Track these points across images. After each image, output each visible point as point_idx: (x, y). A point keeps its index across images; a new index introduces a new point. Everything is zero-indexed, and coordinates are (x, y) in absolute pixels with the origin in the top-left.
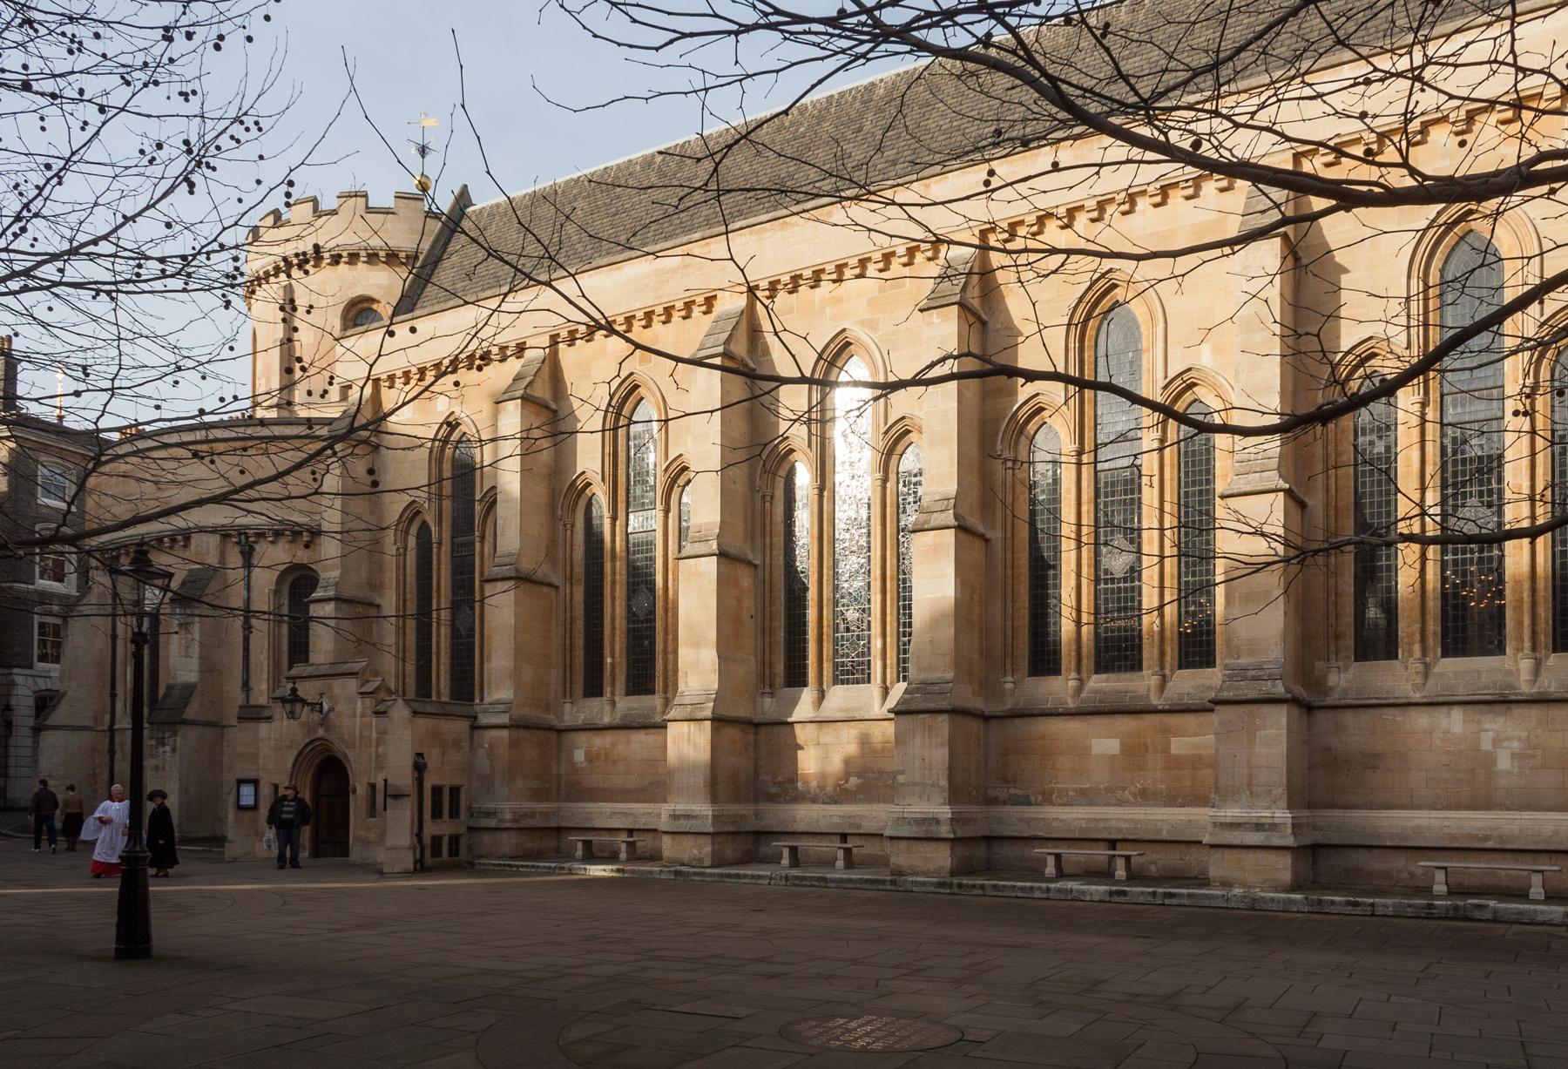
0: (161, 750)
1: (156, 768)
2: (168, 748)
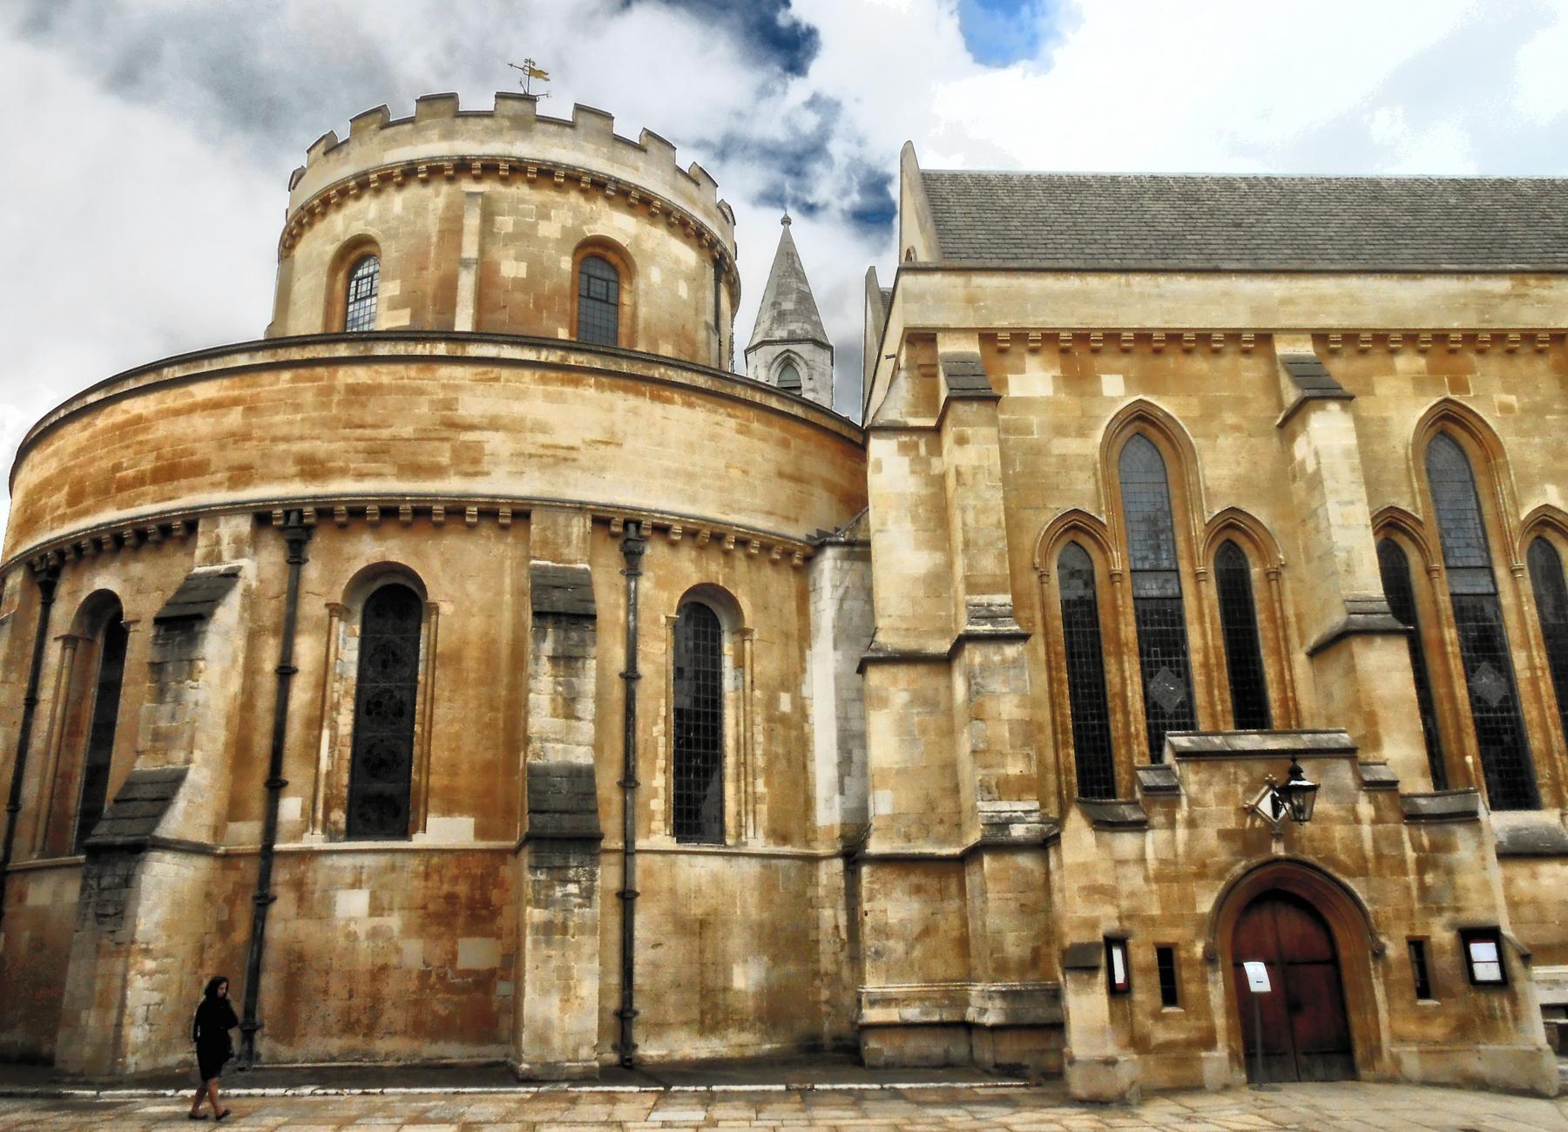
0: (558, 892)
1: (548, 930)
2: (572, 888)
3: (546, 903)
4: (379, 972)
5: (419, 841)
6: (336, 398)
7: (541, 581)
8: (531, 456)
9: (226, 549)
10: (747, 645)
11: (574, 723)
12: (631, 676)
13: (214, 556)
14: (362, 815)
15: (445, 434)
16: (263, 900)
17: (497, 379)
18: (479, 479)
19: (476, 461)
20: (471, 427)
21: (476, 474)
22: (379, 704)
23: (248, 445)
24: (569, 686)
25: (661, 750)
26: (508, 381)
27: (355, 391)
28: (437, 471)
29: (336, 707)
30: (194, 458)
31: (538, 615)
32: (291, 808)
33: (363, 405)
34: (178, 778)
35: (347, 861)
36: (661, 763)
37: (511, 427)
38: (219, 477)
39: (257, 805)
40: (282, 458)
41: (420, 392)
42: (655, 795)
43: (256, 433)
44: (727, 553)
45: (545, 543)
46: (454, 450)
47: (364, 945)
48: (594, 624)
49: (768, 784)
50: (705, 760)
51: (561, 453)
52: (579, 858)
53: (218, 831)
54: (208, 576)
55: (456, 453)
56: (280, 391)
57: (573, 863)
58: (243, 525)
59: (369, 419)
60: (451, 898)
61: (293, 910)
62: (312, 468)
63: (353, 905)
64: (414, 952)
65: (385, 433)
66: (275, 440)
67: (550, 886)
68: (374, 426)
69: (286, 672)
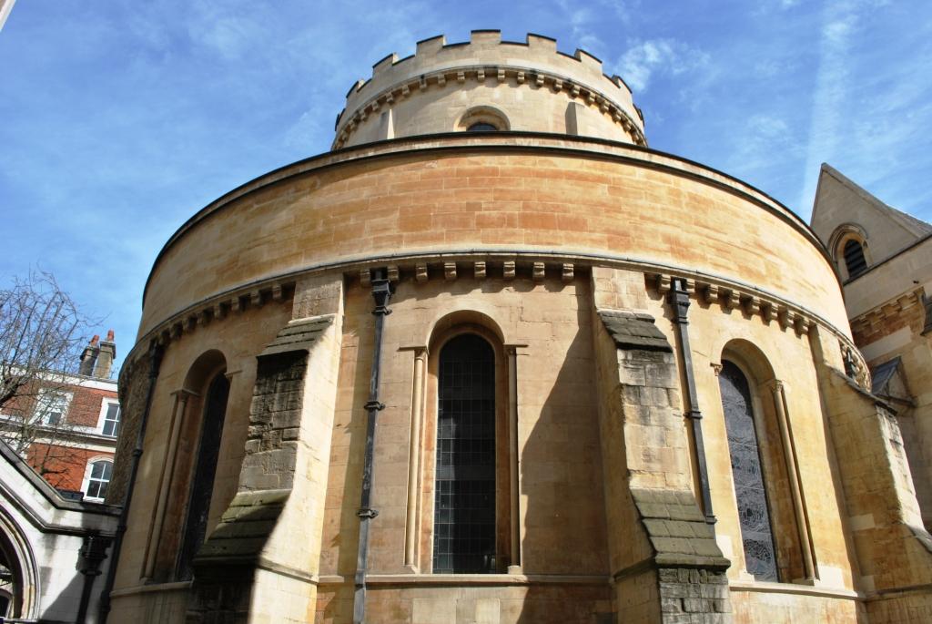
20: (770, 252)
23: (620, 216)
27: (696, 200)
30: (568, 215)
33: (704, 212)
38: (597, 236)
40: (654, 234)
56: (632, 181)
58: (638, 279)
62: (676, 247)
66: (642, 218)
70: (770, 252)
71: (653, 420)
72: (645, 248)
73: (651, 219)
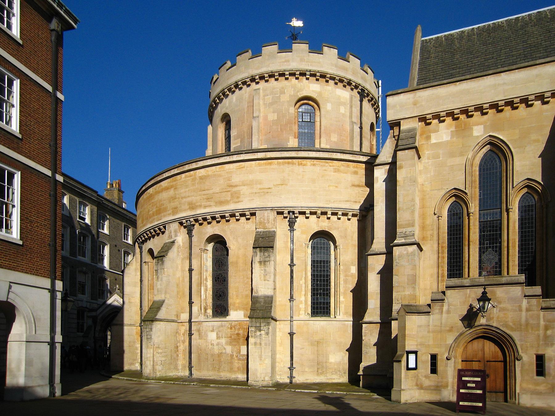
0: (258, 333)
2: (263, 332)
3: (255, 337)
4: (220, 355)
5: (228, 318)
6: (197, 181)
7: (258, 236)
8: (256, 193)
9: (173, 234)
10: (338, 250)
11: (266, 282)
12: (292, 265)
13: (170, 237)
14: (216, 311)
15: (229, 190)
16: (190, 335)
17: (244, 167)
18: (240, 203)
19: (238, 197)
20: (236, 186)
21: (239, 202)
22: (218, 278)
24: (265, 270)
25: (303, 289)
26: (247, 167)
27: (201, 178)
28: (226, 202)
29: (206, 279)
31: (253, 248)
32: (195, 309)
34: (164, 301)
35: (210, 324)
36: (303, 293)
37: (250, 184)
38: (170, 212)
39: (188, 309)
41: (220, 176)
42: (301, 302)
43: (177, 196)
44: (329, 218)
45: (261, 223)
46: (232, 195)
47: (216, 347)
48: (273, 250)
49: (344, 298)
50: (324, 290)
51: (266, 191)
52: (264, 324)
53: (177, 316)
54: (168, 243)
55: (232, 195)
57: (262, 325)
58: (176, 225)
59: (206, 188)
60: (238, 334)
61: (198, 337)
62: (192, 207)
63: (212, 336)
64: (229, 349)
65: (211, 192)
67: (255, 332)
68: (208, 190)
69: (191, 270)
70: (236, 186)
71: (159, 280)
72: (181, 211)
73: (185, 197)
